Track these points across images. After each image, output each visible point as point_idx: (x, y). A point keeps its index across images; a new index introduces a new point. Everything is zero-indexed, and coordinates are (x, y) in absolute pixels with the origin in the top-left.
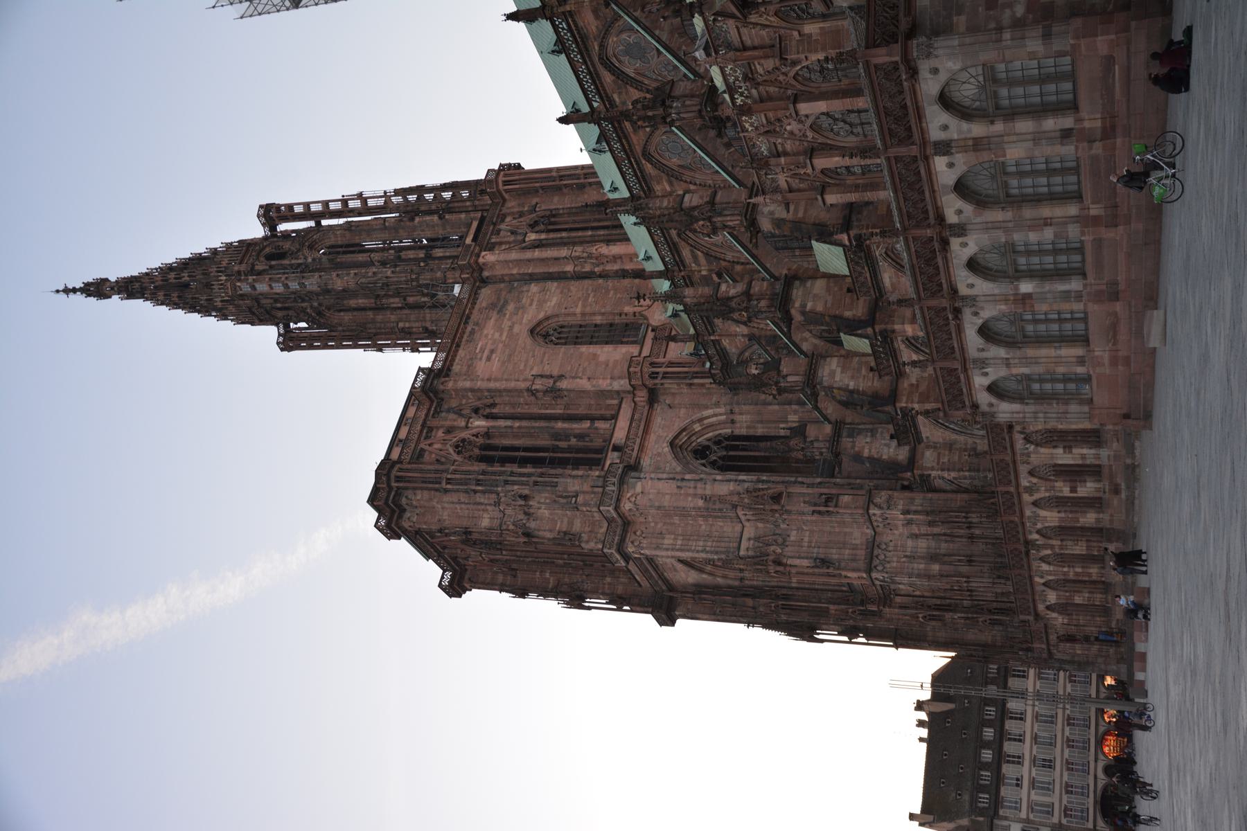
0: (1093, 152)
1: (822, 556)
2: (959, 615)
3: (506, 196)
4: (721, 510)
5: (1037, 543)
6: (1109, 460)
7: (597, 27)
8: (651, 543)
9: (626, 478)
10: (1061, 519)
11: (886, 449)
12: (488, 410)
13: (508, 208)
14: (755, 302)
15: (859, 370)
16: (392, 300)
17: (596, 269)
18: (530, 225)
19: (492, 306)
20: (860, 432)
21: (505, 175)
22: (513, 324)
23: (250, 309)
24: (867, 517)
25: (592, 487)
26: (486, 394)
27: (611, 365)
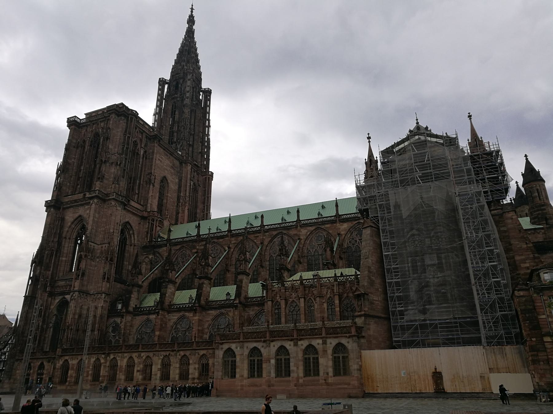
0: (321, 380)
2: (41, 324)
3: (204, 177)
4: (108, 238)
5: (108, 357)
6: (154, 383)
7: (291, 234)
10: (121, 367)
11: (133, 303)
12: (145, 156)
15: (171, 298)
16: (176, 127)
19: (174, 165)
20: (138, 294)
21: (211, 178)
22: (168, 171)
24: (101, 292)
25: (121, 191)
26: (151, 157)
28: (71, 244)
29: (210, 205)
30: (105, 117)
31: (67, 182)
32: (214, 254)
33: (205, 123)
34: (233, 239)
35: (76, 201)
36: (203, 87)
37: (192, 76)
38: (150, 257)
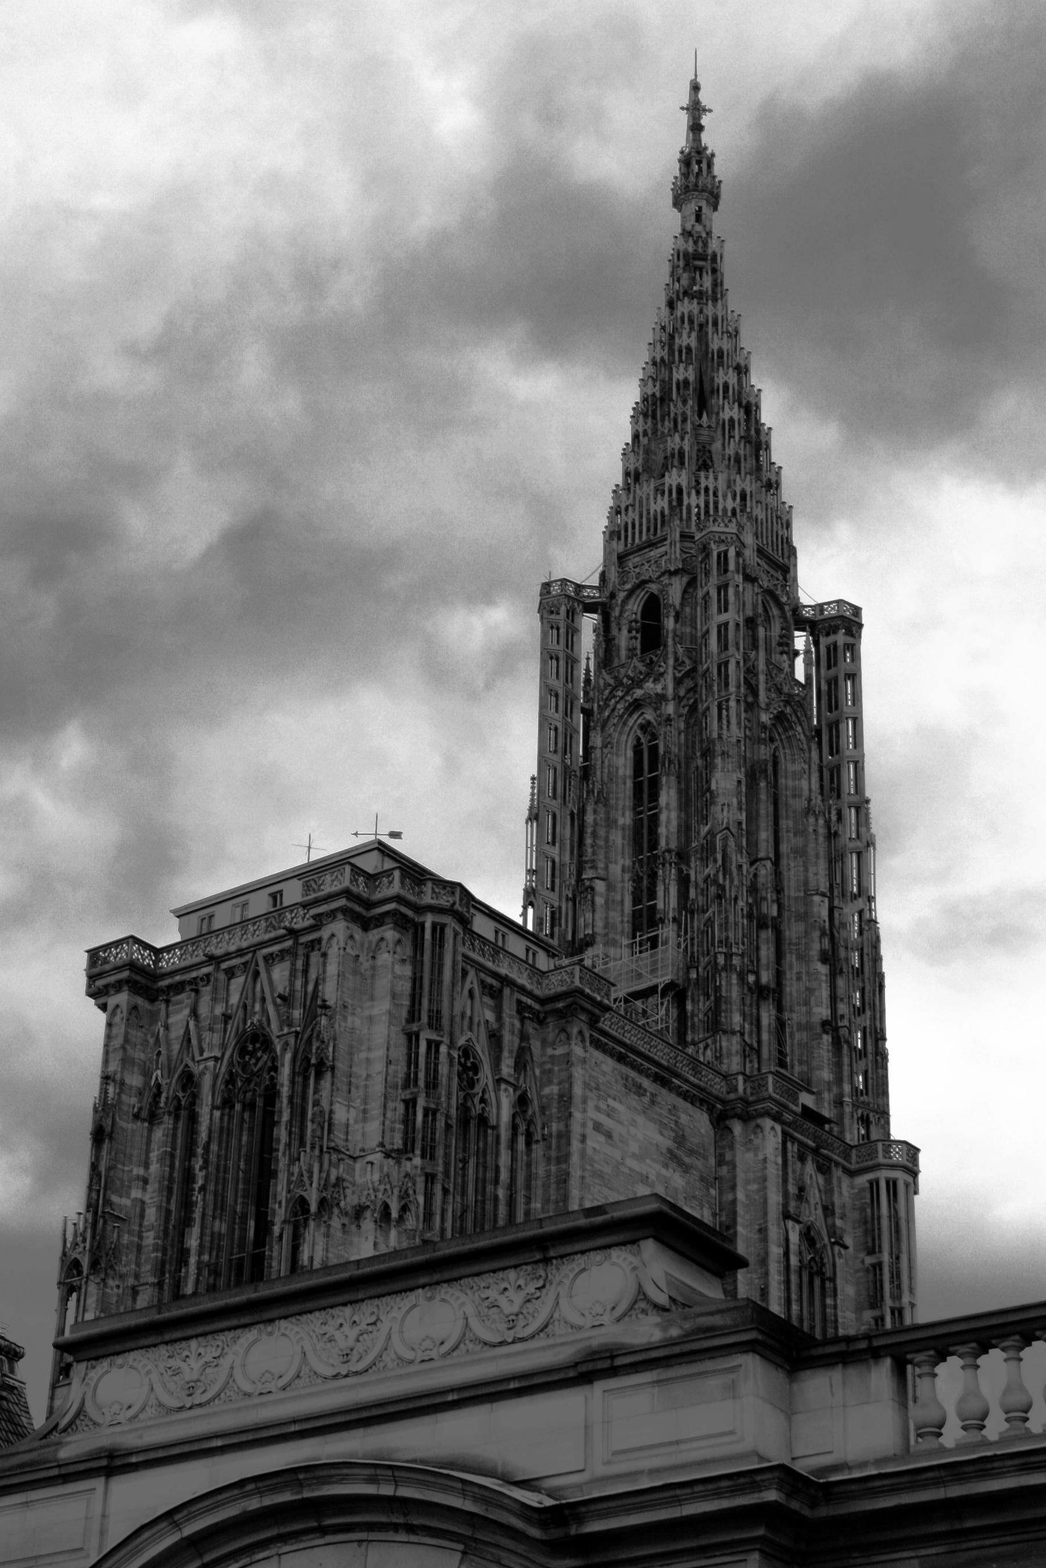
3: (863, 1180)
12: (522, 1128)
13: (839, 1180)
18: (809, 1229)
21: (907, 1185)
26: (555, 1127)
30: (292, 933)
33: (832, 836)
36: (805, 599)
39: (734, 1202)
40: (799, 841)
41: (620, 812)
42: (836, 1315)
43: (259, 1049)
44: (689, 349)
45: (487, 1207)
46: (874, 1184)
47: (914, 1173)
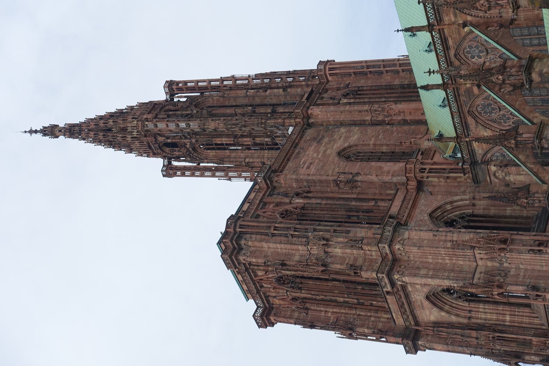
1: (533, 285)
3: (330, 78)
8: (411, 273)
9: (398, 229)
12: (305, 194)
13: (330, 85)
14: (509, 70)
16: (245, 139)
17: (386, 119)
18: (344, 95)
19: (314, 139)
21: (331, 64)
22: (327, 149)
23: (148, 143)
26: (305, 184)
27: (391, 172)
28: (479, 308)
29: (383, 61)
30: (247, 270)
31: (369, 322)
32: (481, 52)
33: (231, 88)
34: (446, 19)
35: (401, 306)
37: (147, 121)
38: (493, 168)
39: (333, 121)
40: (232, 99)
41: (226, 154)
42: (369, 86)
43: (282, 279)
44: (94, 134)
45: (328, 207)
46: (331, 75)
47: (328, 61)
